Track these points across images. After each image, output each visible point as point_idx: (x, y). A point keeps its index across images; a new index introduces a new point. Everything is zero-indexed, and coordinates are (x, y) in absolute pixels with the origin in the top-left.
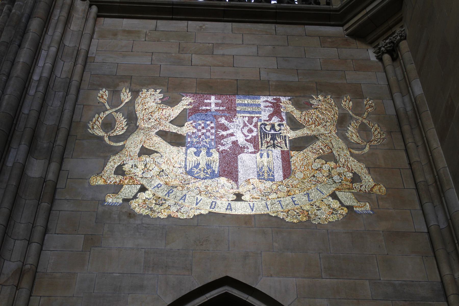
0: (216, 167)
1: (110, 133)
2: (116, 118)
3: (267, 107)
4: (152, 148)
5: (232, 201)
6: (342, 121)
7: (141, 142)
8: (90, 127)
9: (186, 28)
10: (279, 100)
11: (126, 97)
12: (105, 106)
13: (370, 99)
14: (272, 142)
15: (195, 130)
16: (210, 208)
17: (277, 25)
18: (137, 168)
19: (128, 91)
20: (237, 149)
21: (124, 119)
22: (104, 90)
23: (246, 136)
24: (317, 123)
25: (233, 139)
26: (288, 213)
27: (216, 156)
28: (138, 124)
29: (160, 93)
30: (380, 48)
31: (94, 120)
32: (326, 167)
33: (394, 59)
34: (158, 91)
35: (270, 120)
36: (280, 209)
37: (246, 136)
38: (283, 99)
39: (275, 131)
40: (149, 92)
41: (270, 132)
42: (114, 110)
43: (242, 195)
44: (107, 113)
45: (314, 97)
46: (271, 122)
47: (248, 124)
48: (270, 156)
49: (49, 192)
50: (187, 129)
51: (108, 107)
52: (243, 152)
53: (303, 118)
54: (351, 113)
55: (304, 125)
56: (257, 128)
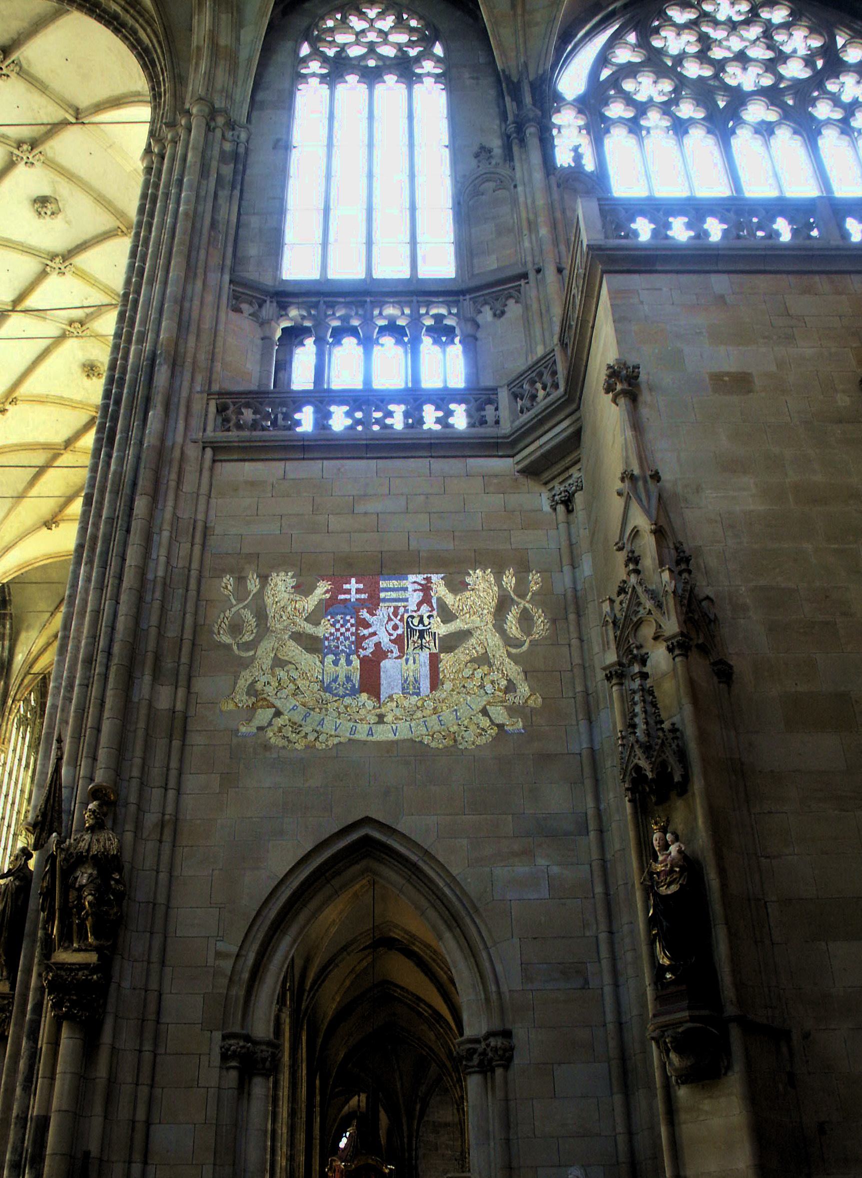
0: (356, 677)
3: (415, 591)
4: (286, 658)
6: (503, 605)
8: (216, 631)
9: (320, 473)
10: (428, 579)
11: (253, 585)
13: (537, 572)
14: (420, 641)
17: (432, 460)
19: (255, 577)
20: (380, 653)
22: (228, 577)
23: (391, 635)
25: (375, 639)
26: (433, 736)
27: (356, 663)
30: (554, 496)
32: (479, 673)
33: (569, 511)
35: (418, 610)
36: (424, 732)
38: (435, 578)
42: (241, 606)
46: (419, 613)
47: (392, 617)
48: (417, 661)
49: (180, 725)
50: (324, 629)
51: (234, 602)
52: (386, 657)
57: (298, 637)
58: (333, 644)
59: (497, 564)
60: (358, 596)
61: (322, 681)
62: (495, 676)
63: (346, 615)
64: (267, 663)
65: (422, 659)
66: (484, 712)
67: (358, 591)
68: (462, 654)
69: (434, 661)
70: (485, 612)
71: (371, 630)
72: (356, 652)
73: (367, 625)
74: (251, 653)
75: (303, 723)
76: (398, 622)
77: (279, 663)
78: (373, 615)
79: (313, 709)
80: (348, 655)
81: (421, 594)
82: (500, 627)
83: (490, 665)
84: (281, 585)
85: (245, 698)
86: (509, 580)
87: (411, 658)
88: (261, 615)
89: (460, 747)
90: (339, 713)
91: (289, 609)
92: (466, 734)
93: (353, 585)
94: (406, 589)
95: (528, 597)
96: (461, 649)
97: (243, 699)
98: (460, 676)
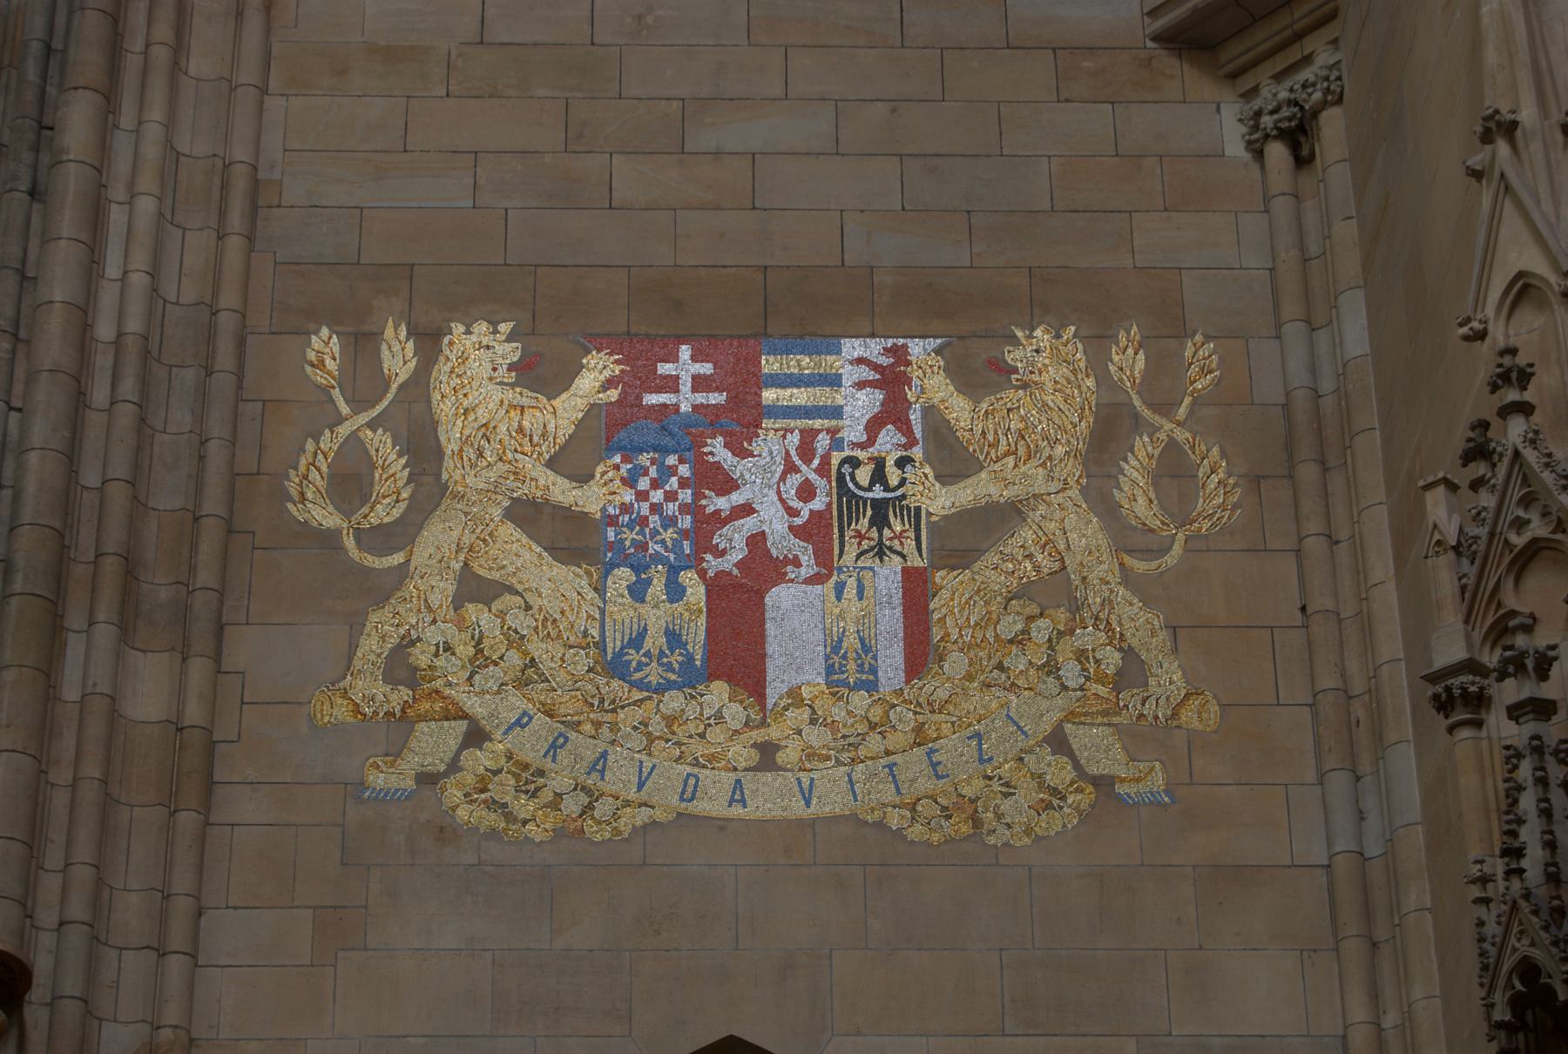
0: (697, 634)
1: (358, 516)
2: (373, 453)
3: (861, 385)
4: (496, 575)
5: (746, 770)
6: (1109, 432)
7: (459, 549)
8: (294, 493)
9: (587, 27)
11: (398, 356)
12: (332, 401)
13: (1208, 338)
14: (874, 534)
15: (628, 496)
16: (682, 799)
18: (453, 654)
20: (763, 567)
21: (400, 455)
22: (325, 332)
23: (792, 512)
24: (1022, 451)
25: (749, 524)
26: (913, 809)
27: (696, 592)
28: (445, 476)
29: (510, 339)
30: (1258, 114)
31: (303, 462)
32: (1042, 630)
33: (1302, 161)
34: (505, 328)
35: (871, 441)
36: (889, 795)
37: (792, 512)
38: (917, 349)
39: (887, 489)
40: (474, 338)
41: (870, 495)
42: (363, 418)
43: (778, 748)
44: (344, 430)
45: (1019, 334)
47: (798, 462)
48: (868, 592)
49: (193, 768)
51: (345, 409)
52: (781, 578)
53: (978, 430)
54: (1137, 402)
55: (982, 458)
56: (830, 482)
57: (530, 514)
58: (630, 536)
59: (1093, 310)
60: (700, 398)
61: (601, 645)
62: (1087, 637)
63: (666, 451)
64: (442, 590)
65: (882, 585)
66: (1058, 742)
67: (699, 383)
68: (994, 571)
69: (916, 588)
70: (1060, 450)
71: (737, 498)
72: (696, 562)
73: (728, 485)
74: (398, 558)
75: (548, 764)
76: (813, 476)
77: (475, 589)
78: (742, 453)
80: (673, 571)
81: (879, 396)
82: (1104, 506)
83: (1076, 607)
84: (480, 356)
85: (380, 689)
86: (1129, 360)
88: (423, 449)
89: (991, 840)
90: (651, 739)
91: (503, 428)
92: (1006, 806)
93: (685, 365)
94: (834, 381)
95: (1182, 412)
96: (992, 558)
97: (372, 689)
98: (990, 634)
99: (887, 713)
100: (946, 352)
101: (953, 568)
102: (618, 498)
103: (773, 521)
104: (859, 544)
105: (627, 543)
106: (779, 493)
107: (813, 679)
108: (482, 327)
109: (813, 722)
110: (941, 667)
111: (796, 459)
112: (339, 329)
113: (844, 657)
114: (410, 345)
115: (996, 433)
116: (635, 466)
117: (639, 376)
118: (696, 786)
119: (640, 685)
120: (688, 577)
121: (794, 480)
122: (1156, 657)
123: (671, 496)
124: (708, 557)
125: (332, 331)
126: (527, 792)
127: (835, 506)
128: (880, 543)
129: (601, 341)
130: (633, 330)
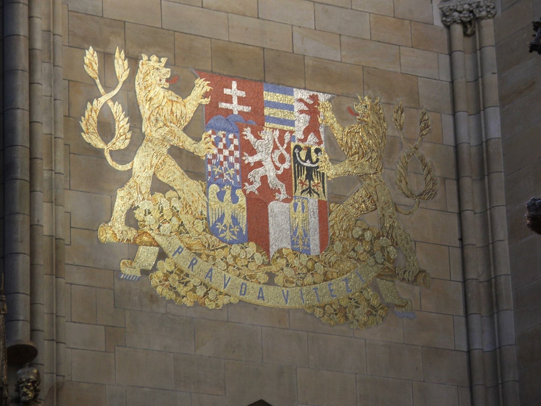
2: (114, 113)
3: (301, 112)
7: (152, 166)
8: (84, 128)
12: (97, 85)
16: (241, 294)
19: (123, 56)
20: (266, 193)
21: (125, 116)
23: (278, 168)
24: (361, 153)
25: (261, 171)
26: (324, 309)
27: (242, 201)
28: (143, 130)
29: (166, 66)
32: (368, 235)
34: (164, 60)
37: (278, 168)
39: (312, 163)
45: (359, 97)
46: (307, 144)
47: (279, 145)
50: (204, 148)
51: (102, 90)
52: (273, 198)
56: (290, 156)
57: (177, 153)
58: (217, 170)
61: (207, 219)
62: (383, 241)
63: (229, 132)
67: (241, 101)
72: (242, 186)
74: (128, 167)
75: (191, 272)
76: (284, 152)
79: (200, 255)
80: (234, 189)
81: (308, 118)
87: (300, 204)
90: (228, 265)
92: (356, 312)
99: (314, 265)
100: (333, 101)
101: (336, 203)
102: (211, 151)
103: (269, 171)
104: (302, 186)
105: (216, 173)
106: (272, 158)
107: (286, 245)
108: (154, 58)
109: (287, 265)
110: (333, 247)
111: (277, 143)
112: (98, 49)
113: (298, 238)
114: (126, 62)
115: (351, 144)
116: (217, 137)
117: (217, 95)
118: (246, 289)
119: (222, 240)
120: (239, 192)
121: (277, 153)
122: (409, 253)
123: (231, 153)
124: (246, 184)
125: (94, 50)
126: (183, 283)
127: (293, 168)
128: (310, 187)
129: (201, 73)
130: (214, 71)
